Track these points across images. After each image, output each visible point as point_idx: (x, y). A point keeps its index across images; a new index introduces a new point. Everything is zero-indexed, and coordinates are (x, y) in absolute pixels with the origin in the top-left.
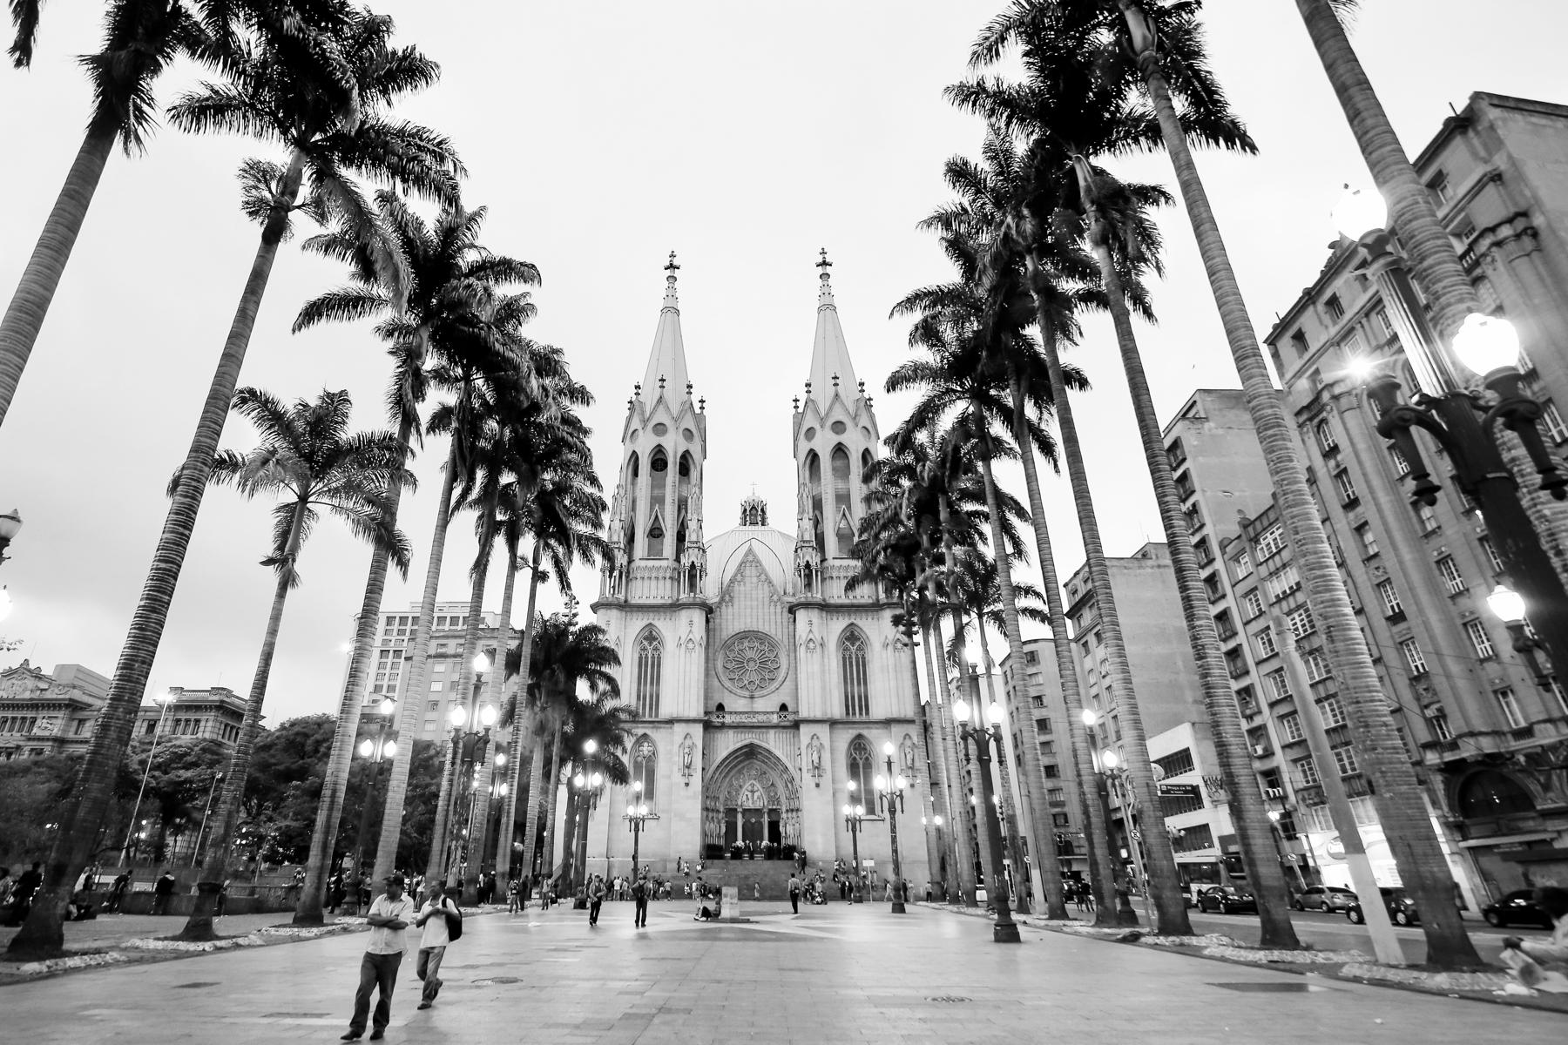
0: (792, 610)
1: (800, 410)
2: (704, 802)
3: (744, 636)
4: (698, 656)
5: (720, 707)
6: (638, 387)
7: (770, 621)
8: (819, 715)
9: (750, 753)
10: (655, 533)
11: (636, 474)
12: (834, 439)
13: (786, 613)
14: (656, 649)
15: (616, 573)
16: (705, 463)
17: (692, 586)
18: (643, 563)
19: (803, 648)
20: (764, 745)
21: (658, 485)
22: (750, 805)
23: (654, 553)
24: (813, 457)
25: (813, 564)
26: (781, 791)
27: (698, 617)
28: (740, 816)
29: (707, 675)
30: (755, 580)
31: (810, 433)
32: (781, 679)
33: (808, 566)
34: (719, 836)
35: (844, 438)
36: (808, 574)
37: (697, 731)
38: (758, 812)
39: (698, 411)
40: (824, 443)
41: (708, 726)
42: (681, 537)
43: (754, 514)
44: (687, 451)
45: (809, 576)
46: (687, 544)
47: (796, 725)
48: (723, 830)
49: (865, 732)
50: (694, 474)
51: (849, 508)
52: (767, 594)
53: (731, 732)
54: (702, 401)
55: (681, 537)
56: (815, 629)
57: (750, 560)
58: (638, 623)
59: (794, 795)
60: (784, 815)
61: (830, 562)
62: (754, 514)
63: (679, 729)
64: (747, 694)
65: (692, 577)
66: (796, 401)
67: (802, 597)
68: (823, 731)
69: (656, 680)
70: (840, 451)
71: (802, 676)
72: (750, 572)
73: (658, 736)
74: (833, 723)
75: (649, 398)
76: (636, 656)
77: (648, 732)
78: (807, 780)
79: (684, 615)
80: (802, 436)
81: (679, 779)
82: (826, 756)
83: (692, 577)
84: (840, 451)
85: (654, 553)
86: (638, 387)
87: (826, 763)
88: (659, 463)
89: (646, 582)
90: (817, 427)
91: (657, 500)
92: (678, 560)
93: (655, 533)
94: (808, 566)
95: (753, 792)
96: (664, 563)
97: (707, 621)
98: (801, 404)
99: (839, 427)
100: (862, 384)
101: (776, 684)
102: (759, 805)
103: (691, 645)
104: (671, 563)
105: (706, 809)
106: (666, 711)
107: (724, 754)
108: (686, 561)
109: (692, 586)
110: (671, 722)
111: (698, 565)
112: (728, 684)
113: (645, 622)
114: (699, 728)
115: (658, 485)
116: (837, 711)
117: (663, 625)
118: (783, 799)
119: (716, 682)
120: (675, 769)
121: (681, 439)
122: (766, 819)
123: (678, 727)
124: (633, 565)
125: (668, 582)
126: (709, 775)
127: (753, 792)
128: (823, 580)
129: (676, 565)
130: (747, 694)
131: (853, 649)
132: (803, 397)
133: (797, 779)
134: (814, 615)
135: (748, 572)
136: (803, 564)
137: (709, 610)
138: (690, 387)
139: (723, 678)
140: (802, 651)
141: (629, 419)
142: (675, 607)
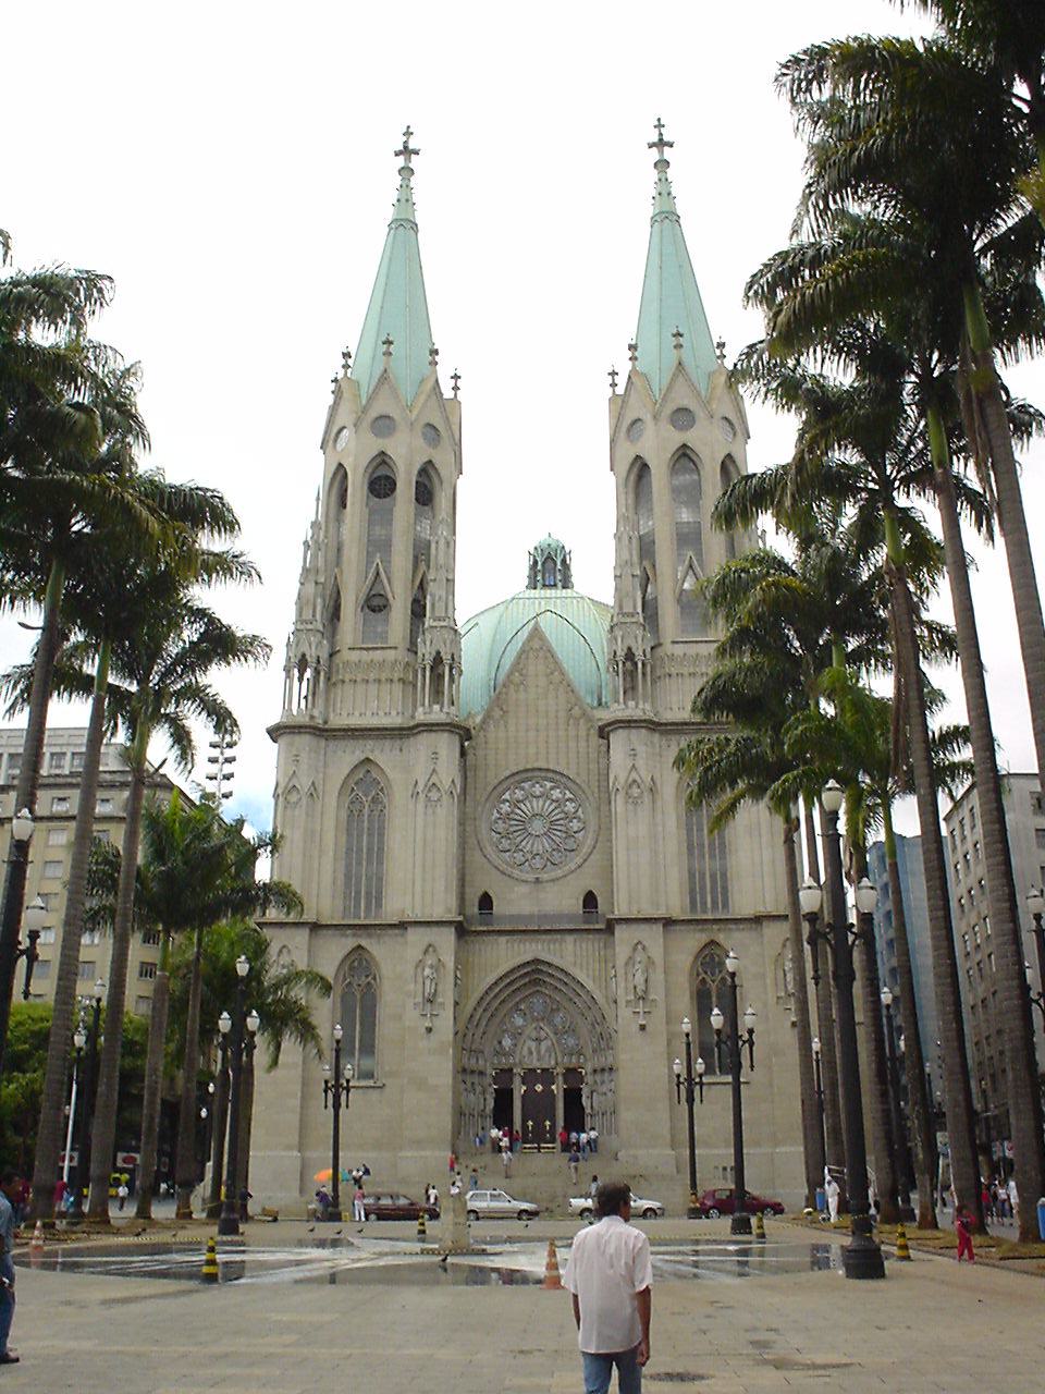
0: (604, 732)
1: (620, 390)
2: (457, 1059)
4: (445, 815)
5: (486, 902)
6: (347, 355)
7: (569, 753)
8: (649, 912)
9: (534, 975)
10: (376, 604)
11: (343, 505)
12: (676, 438)
13: (595, 740)
14: (375, 800)
15: (308, 674)
16: (461, 483)
17: (437, 693)
18: (354, 656)
19: (620, 798)
20: (556, 961)
21: (379, 519)
22: (535, 1064)
23: (372, 640)
24: (640, 469)
25: (638, 653)
27: (446, 745)
28: (517, 1081)
30: (543, 681)
32: (585, 850)
33: (630, 655)
34: (482, 1115)
35: (692, 437)
36: (631, 669)
37: (446, 940)
38: (547, 1076)
39: (448, 393)
40: (657, 446)
41: (462, 931)
42: (418, 611)
43: (550, 568)
44: (430, 462)
45: (630, 676)
46: (428, 622)
47: (610, 927)
48: (491, 1104)
49: (721, 938)
50: (441, 500)
51: (699, 554)
53: (503, 939)
54: (456, 377)
55: (418, 611)
56: (640, 763)
57: (536, 646)
58: (346, 757)
59: (605, 1040)
60: (589, 1079)
61: (668, 648)
62: (550, 568)
63: (417, 937)
65: (437, 678)
66: (613, 374)
67: (617, 711)
68: (653, 937)
69: (378, 853)
70: (685, 456)
71: (620, 846)
72: (535, 668)
73: (377, 948)
74: (668, 922)
75: (364, 373)
76: (344, 814)
77: (363, 943)
78: (625, 1020)
79: (425, 739)
81: (413, 1017)
82: (658, 977)
83: (437, 678)
84: (685, 456)
85: (372, 640)
86: (347, 355)
87: (657, 994)
88: (381, 484)
89: (361, 688)
90: (648, 418)
91: (378, 546)
92: (413, 649)
93: (376, 604)
94: (630, 655)
96: (390, 655)
97: (463, 753)
98: (622, 381)
99: (683, 418)
100: (721, 345)
102: (549, 1063)
103: (434, 795)
104: (401, 655)
105: (463, 1071)
106: (396, 905)
107: (491, 979)
108: (426, 650)
109: (437, 693)
110: (403, 926)
111: (446, 657)
113: (359, 756)
114: (449, 936)
115: (379, 519)
116: (675, 905)
117: (385, 755)
118: (588, 1052)
121: (420, 442)
122: (558, 1088)
123: (413, 935)
124: (337, 659)
125: (398, 688)
128: (654, 682)
129: (408, 657)
130: (531, 877)
132: (624, 369)
133: (609, 1013)
134: (639, 737)
135: (531, 668)
136: (621, 654)
137: (464, 733)
138: (436, 352)
139: (489, 850)
140: (619, 804)
141: (334, 409)
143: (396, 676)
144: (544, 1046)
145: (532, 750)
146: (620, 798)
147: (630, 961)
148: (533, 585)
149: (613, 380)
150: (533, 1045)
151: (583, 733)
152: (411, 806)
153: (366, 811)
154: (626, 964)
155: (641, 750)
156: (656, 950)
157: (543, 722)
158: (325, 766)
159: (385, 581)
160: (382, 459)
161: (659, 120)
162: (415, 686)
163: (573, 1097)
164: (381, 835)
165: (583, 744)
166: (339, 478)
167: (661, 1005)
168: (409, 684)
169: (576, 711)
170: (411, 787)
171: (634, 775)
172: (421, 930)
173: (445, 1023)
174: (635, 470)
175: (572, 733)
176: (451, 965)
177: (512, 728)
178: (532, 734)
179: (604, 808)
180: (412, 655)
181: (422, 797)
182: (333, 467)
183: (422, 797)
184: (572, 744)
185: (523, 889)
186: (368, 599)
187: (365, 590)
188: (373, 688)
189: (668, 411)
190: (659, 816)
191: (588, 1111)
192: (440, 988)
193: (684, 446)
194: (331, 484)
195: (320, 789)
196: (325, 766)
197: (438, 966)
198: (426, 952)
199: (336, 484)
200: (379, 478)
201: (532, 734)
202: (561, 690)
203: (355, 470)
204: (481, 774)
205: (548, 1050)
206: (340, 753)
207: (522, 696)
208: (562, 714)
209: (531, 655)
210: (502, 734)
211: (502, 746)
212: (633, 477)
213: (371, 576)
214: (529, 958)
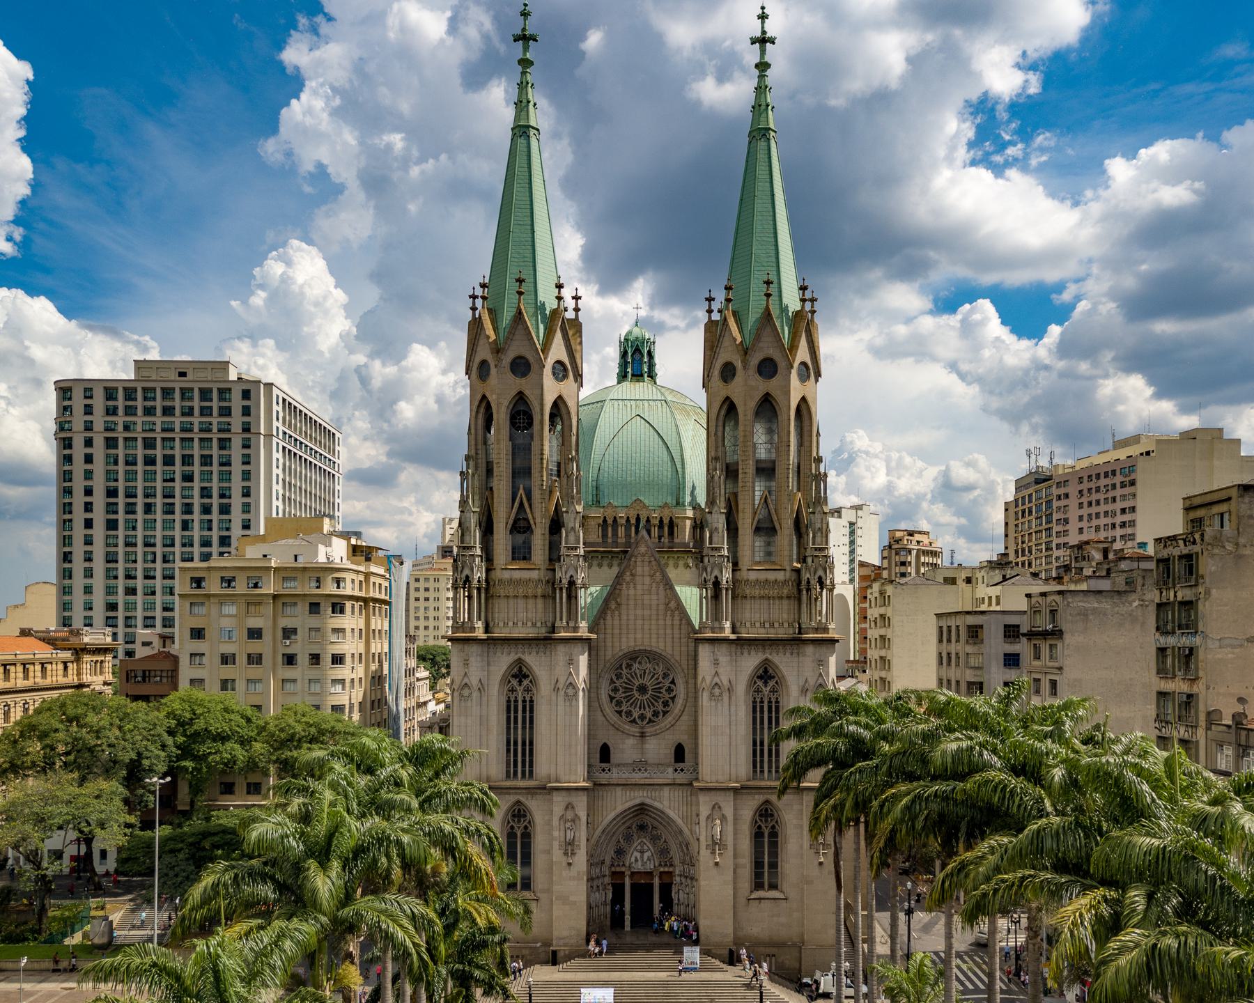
3: (633, 656)
12: (762, 386)
19: (706, 695)
20: (657, 804)
22: (639, 867)
26: (675, 852)
29: (589, 706)
30: (647, 580)
31: (728, 372)
40: (747, 389)
48: (610, 896)
52: (662, 601)
54: (576, 298)
56: (721, 671)
58: (503, 661)
60: (678, 879)
63: (559, 800)
64: (634, 729)
76: (504, 699)
80: (716, 372)
81: (557, 854)
95: (642, 852)
96: (534, 575)
101: (670, 719)
102: (650, 866)
112: (614, 718)
117: (534, 660)
118: (677, 861)
119: (600, 718)
120: (556, 844)
122: (657, 881)
125: (540, 601)
126: (593, 841)
127: (642, 852)
131: (766, 690)
134: (723, 654)
135: (639, 569)
140: (705, 698)
142: (546, 641)
143: (539, 591)
144: (646, 855)
145: (639, 636)
146: (706, 695)
147: (710, 818)
148: (622, 377)
149: (710, 306)
150: (638, 855)
151: (677, 622)
152: (554, 698)
153: (520, 699)
154: (708, 818)
155: (724, 659)
156: (728, 811)
157: (647, 613)
158: (489, 664)
159: (528, 510)
160: (521, 397)
161: (763, 8)
162: (554, 598)
163: (666, 889)
164: (532, 710)
165: (676, 631)
166: (484, 405)
167: (730, 848)
168: (549, 597)
169: (673, 605)
170: (553, 682)
171: (716, 680)
172: (564, 793)
173: (581, 859)
174: (725, 407)
175: (669, 622)
176: (584, 819)
177: (624, 617)
178: (639, 622)
179: (691, 681)
180: (550, 573)
181: (562, 693)
182: (479, 397)
183: (562, 693)
184: (669, 631)
185: (631, 742)
186: (515, 521)
187: (513, 516)
188: (521, 602)
189: (755, 360)
190: (733, 708)
191: (676, 901)
192: (577, 834)
193: (768, 394)
194: (477, 412)
195: (485, 683)
196: (489, 664)
197: (575, 819)
198: (567, 808)
199: (482, 410)
200: (518, 413)
201: (639, 622)
202: (661, 588)
203: (499, 404)
204: (601, 653)
205: (649, 859)
206: (499, 654)
207: (632, 592)
208: (662, 607)
209: (639, 559)
210: (616, 622)
211: (616, 631)
212: (723, 413)
213: (516, 504)
214: (638, 801)
